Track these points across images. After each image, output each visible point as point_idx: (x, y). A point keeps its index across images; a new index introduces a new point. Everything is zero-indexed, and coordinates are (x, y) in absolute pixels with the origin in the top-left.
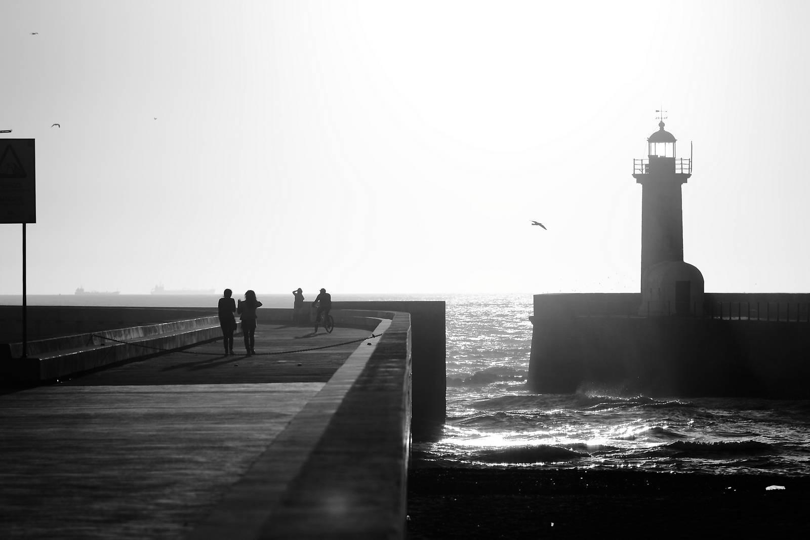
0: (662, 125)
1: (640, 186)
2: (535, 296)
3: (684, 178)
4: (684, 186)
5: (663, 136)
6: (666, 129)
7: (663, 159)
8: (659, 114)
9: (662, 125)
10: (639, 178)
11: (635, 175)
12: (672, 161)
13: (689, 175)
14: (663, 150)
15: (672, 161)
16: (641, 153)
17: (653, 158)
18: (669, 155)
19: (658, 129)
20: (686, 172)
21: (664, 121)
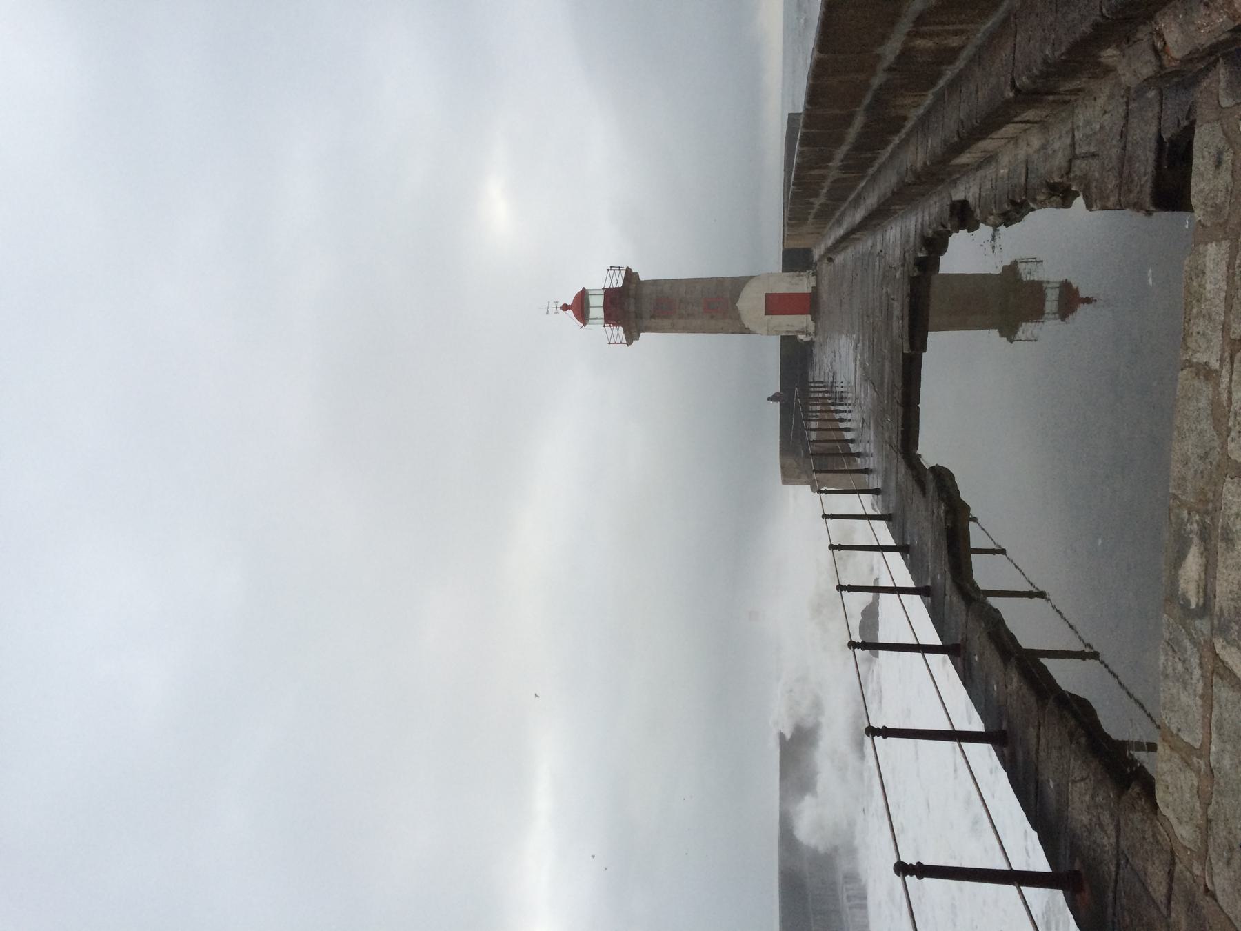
0: (565, 307)
3: (630, 276)
4: (642, 278)
5: (580, 307)
6: (570, 302)
7: (605, 307)
8: (552, 311)
9: (565, 307)
10: (631, 337)
11: (629, 343)
13: (628, 270)
16: (599, 332)
18: (602, 298)
19: (570, 312)
20: (623, 273)
21: (560, 305)
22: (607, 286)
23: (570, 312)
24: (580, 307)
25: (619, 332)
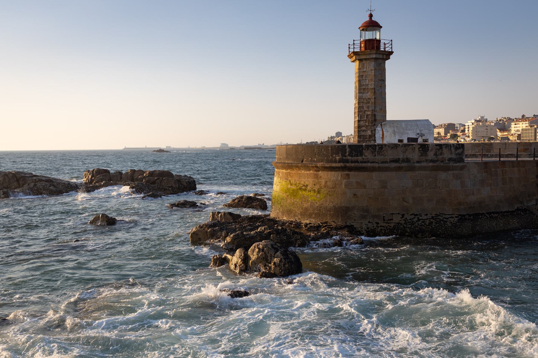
5: (372, 25)
6: (373, 19)
12: (379, 41)
20: (390, 50)
22: (382, 42)
23: (368, 19)
24: (372, 25)
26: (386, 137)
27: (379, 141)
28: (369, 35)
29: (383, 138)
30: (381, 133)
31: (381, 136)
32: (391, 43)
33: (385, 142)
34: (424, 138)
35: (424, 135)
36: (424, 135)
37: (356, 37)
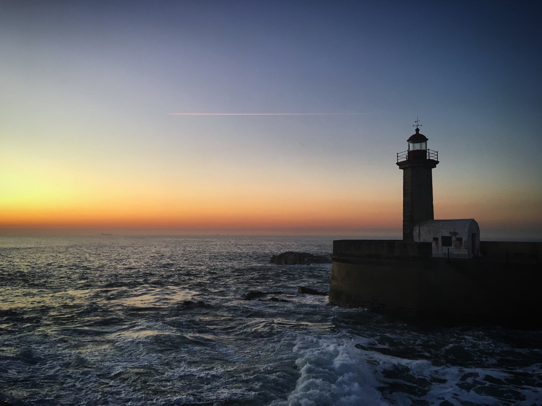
0: (417, 130)
1: (402, 170)
2: (334, 242)
3: (434, 163)
4: (433, 169)
5: (418, 138)
6: (420, 132)
9: (417, 130)
10: (401, 165)
11: (398, 164)
13: (437, 162)
14: (418, 147)
15: (425, 151)
17: (410, 153)
19: (415, 133)
20: (436, 160)
21: (419, 127)
24: (418, 138)
25: (403, 159)
26: (423, 235)
27: (416, 240)
28: (418, 147)
29: (419, 236)
30: (418, 231)
31: (418, 235)
32: (436, 154)
33: (422, 241)
34: (458, 236)
35: (457, 234)
36: (457, 234)
37: (403, 150)
